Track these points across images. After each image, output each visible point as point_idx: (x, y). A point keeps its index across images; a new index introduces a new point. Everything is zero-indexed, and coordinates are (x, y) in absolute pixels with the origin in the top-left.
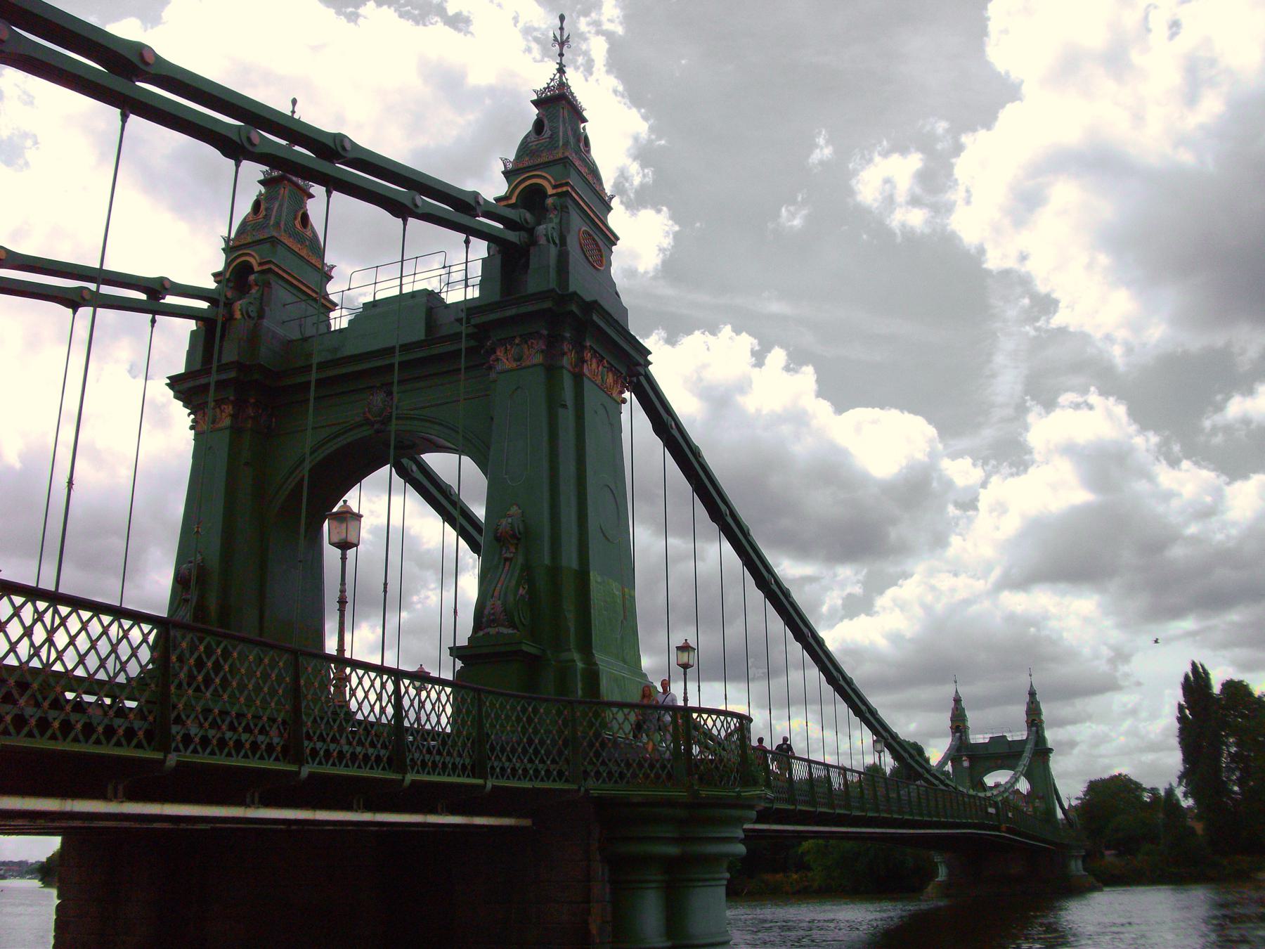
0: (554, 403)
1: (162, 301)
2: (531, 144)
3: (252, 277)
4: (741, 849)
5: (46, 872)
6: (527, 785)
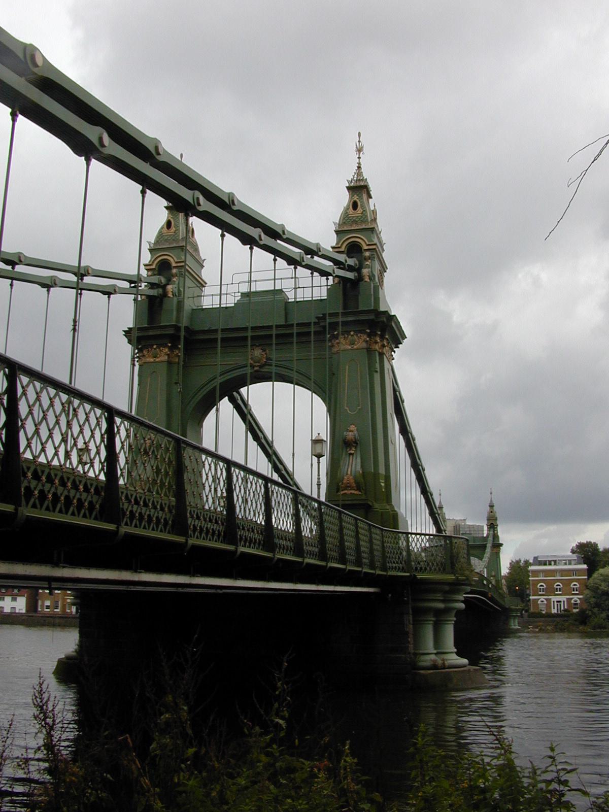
2: (350, 216)
4: (463, 606)
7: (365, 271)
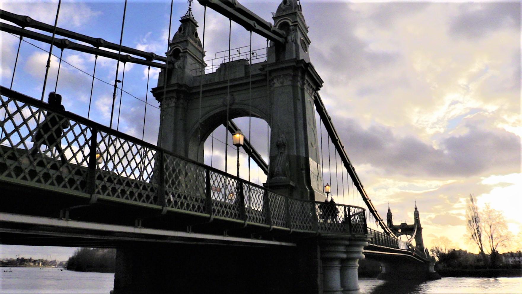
0: (295, 98)
1: (152, 61)
3: (180, 54)
4: (364, 256)
5: (482, 253)
6: (302, 231)
7: (289, 38)
